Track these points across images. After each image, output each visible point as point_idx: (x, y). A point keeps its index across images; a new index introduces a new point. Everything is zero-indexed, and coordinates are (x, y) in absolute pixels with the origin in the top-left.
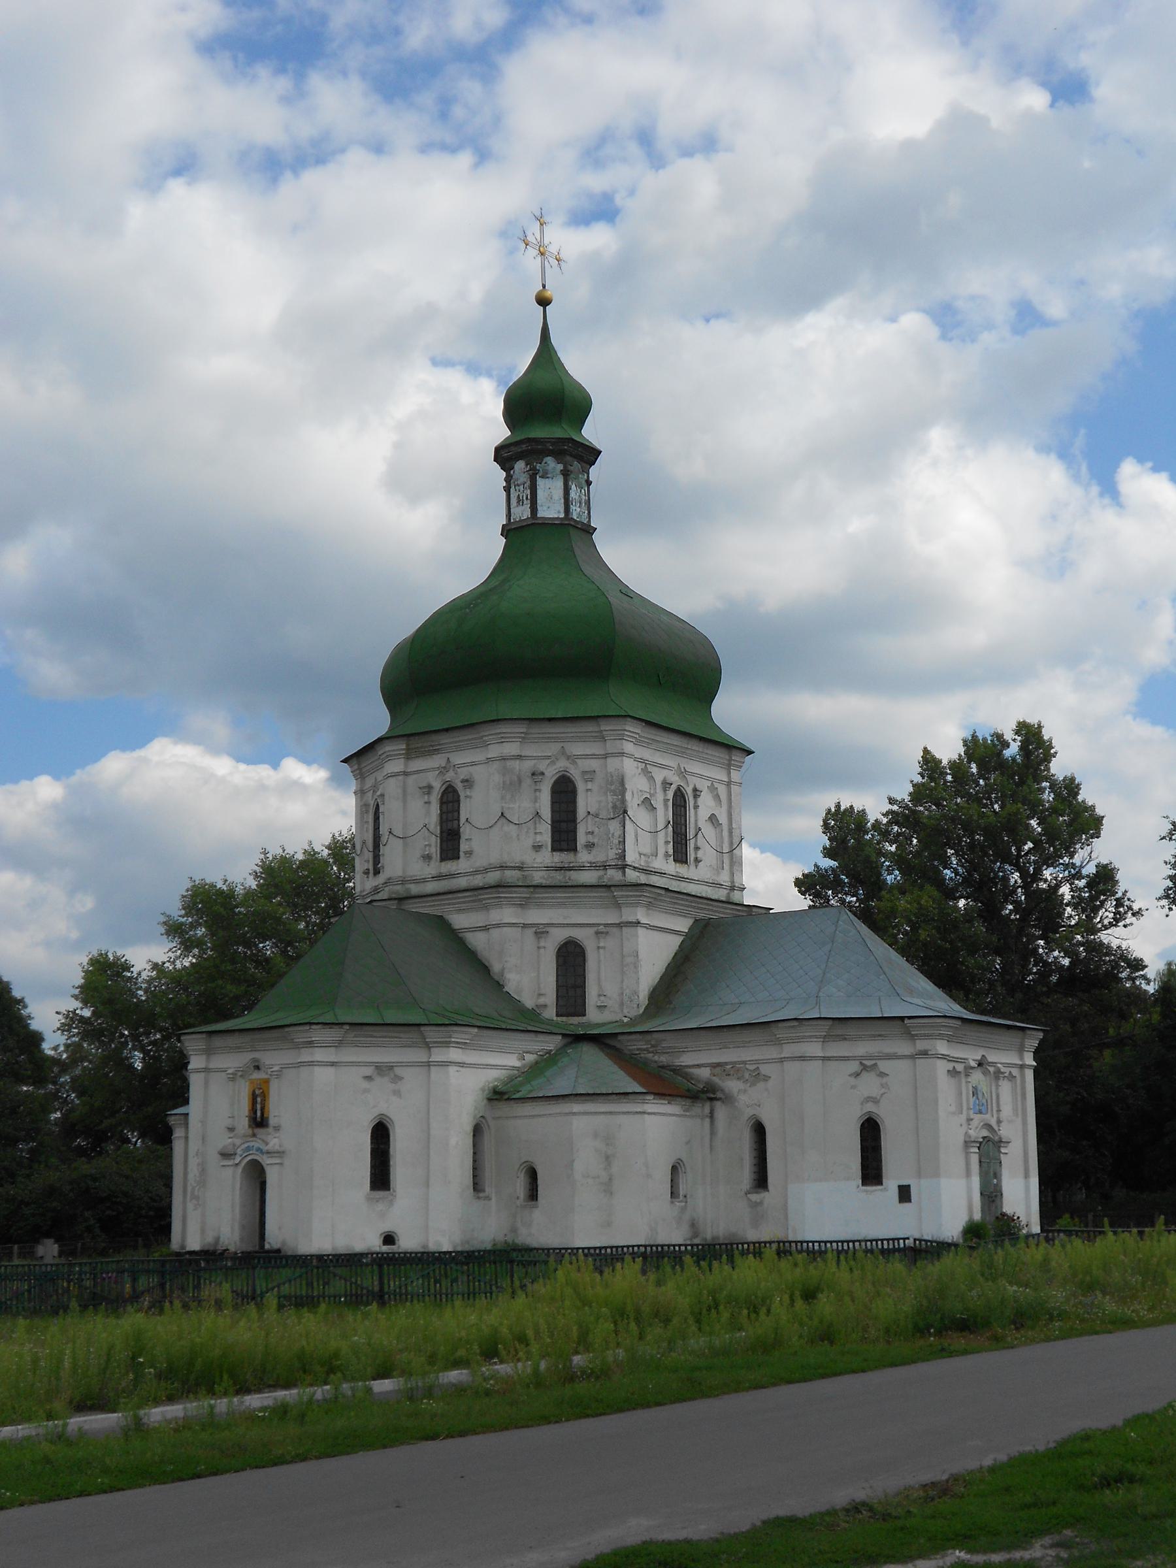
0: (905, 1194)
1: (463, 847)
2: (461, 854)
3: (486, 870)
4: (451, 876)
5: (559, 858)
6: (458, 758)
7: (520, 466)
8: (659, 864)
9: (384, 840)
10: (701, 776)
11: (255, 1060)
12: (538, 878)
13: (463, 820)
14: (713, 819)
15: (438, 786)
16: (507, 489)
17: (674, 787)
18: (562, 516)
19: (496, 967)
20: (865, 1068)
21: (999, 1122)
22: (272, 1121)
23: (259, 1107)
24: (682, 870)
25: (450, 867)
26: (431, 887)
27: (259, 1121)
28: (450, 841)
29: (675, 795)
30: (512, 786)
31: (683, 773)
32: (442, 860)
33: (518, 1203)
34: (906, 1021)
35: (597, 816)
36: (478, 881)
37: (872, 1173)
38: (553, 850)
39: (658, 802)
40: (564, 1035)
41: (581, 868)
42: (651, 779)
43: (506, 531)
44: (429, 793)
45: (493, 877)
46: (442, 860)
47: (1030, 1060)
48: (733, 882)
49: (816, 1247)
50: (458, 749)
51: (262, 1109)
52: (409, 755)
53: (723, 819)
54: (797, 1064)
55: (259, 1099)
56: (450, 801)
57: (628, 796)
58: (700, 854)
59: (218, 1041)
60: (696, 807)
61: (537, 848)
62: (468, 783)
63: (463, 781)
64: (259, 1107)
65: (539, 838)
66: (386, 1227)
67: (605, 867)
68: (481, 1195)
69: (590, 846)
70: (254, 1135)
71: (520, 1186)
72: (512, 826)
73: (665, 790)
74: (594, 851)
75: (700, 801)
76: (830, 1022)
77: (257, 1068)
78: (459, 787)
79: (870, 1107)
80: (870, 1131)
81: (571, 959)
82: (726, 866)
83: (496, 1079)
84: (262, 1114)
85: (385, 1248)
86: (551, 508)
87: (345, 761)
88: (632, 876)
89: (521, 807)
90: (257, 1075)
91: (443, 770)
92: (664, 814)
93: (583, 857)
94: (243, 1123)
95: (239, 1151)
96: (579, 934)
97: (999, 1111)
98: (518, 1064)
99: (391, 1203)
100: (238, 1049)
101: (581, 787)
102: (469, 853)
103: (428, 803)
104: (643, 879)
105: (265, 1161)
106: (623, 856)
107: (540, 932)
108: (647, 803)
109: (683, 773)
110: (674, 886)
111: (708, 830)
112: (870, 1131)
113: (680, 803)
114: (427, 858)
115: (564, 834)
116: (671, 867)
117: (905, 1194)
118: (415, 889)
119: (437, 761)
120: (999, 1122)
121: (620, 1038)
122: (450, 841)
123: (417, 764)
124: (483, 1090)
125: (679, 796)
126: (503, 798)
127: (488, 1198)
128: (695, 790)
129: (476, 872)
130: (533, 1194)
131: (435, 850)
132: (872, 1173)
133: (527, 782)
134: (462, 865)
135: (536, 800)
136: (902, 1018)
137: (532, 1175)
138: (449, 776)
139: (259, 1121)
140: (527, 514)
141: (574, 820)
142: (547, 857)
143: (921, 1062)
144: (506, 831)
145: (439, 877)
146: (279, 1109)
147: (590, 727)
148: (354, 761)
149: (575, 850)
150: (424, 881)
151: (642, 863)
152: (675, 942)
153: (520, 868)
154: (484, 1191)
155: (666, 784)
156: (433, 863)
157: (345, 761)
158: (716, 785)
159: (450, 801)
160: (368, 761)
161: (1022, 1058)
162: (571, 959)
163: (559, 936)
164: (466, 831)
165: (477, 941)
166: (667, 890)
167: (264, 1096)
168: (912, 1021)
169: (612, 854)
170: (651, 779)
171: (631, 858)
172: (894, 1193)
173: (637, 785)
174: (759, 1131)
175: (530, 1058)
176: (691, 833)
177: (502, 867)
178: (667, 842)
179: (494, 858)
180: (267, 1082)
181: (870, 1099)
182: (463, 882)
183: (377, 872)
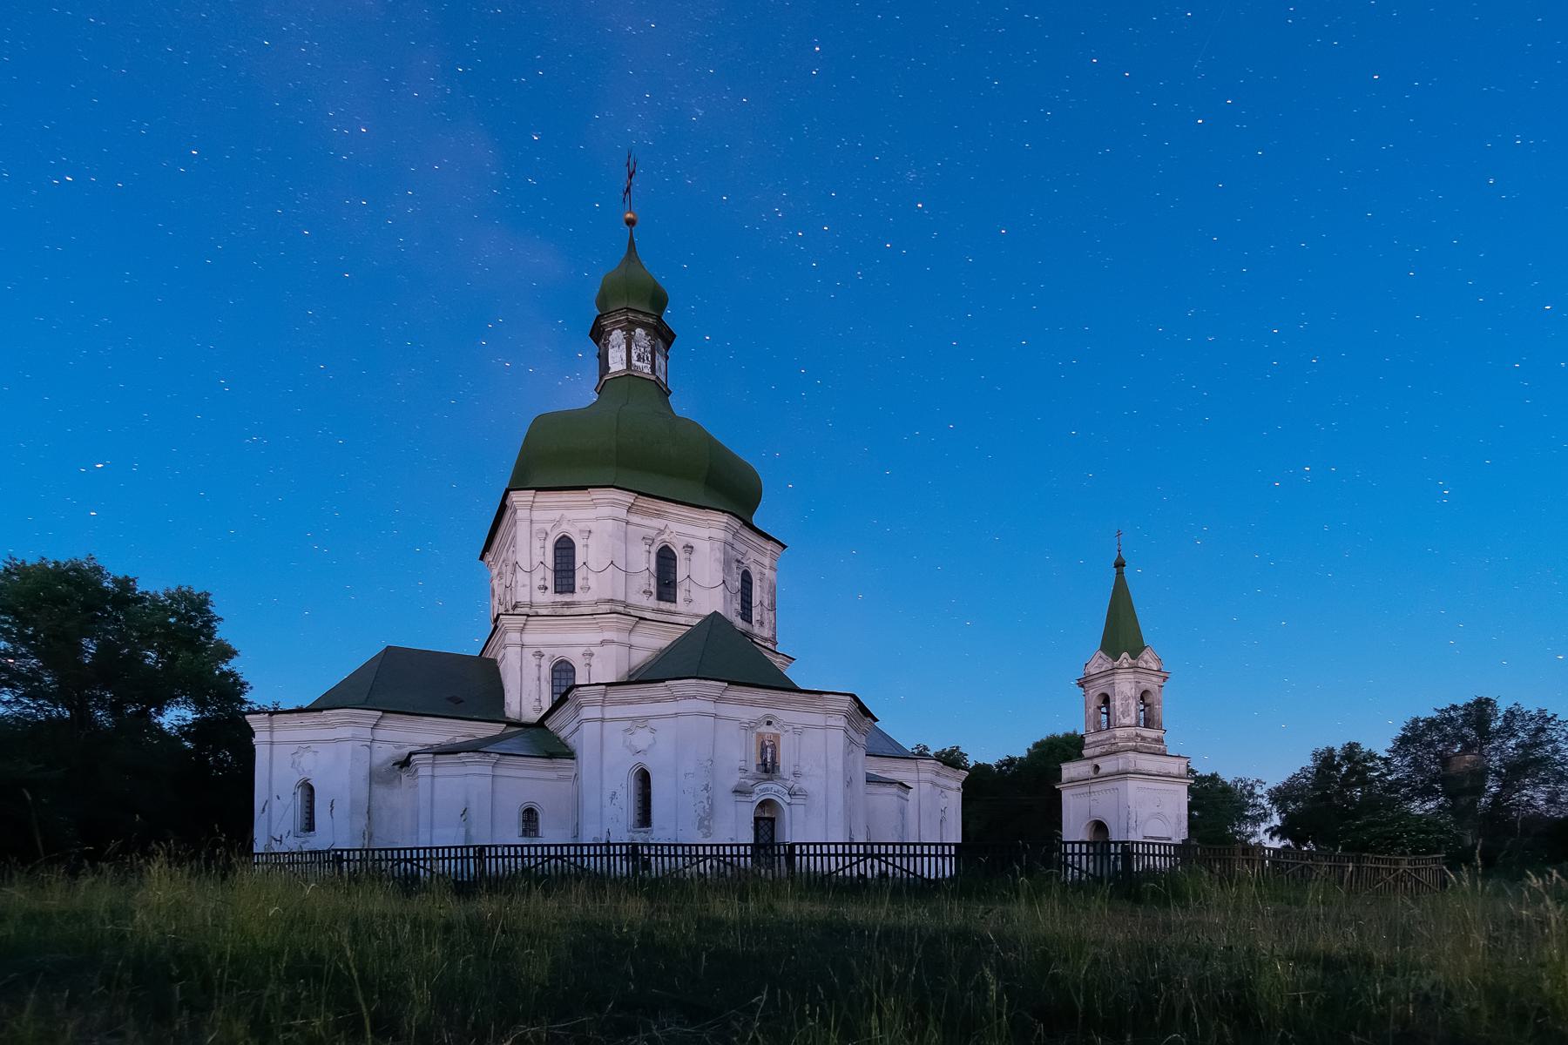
6: (674, 527)
11: (768, 716)
26: (647, 615)
50: (679, 521)
51: (773, 759)
62: (689, 548)
77: (769, 723)
84: (773, 759)
90: (764, 729)
91: (661, 532)
94: (754, 769)
95: (757, 789)
100: (753, 703)
105: (783, 800)
114: (648, 593)
119: (658, 523)
123: (634, 519)
131: (654, 590)
139: (769, 768)
142: (739, 623)
150: (643, 609)
167: (774, 747)
180: (777, 736)
182: (681, 620)
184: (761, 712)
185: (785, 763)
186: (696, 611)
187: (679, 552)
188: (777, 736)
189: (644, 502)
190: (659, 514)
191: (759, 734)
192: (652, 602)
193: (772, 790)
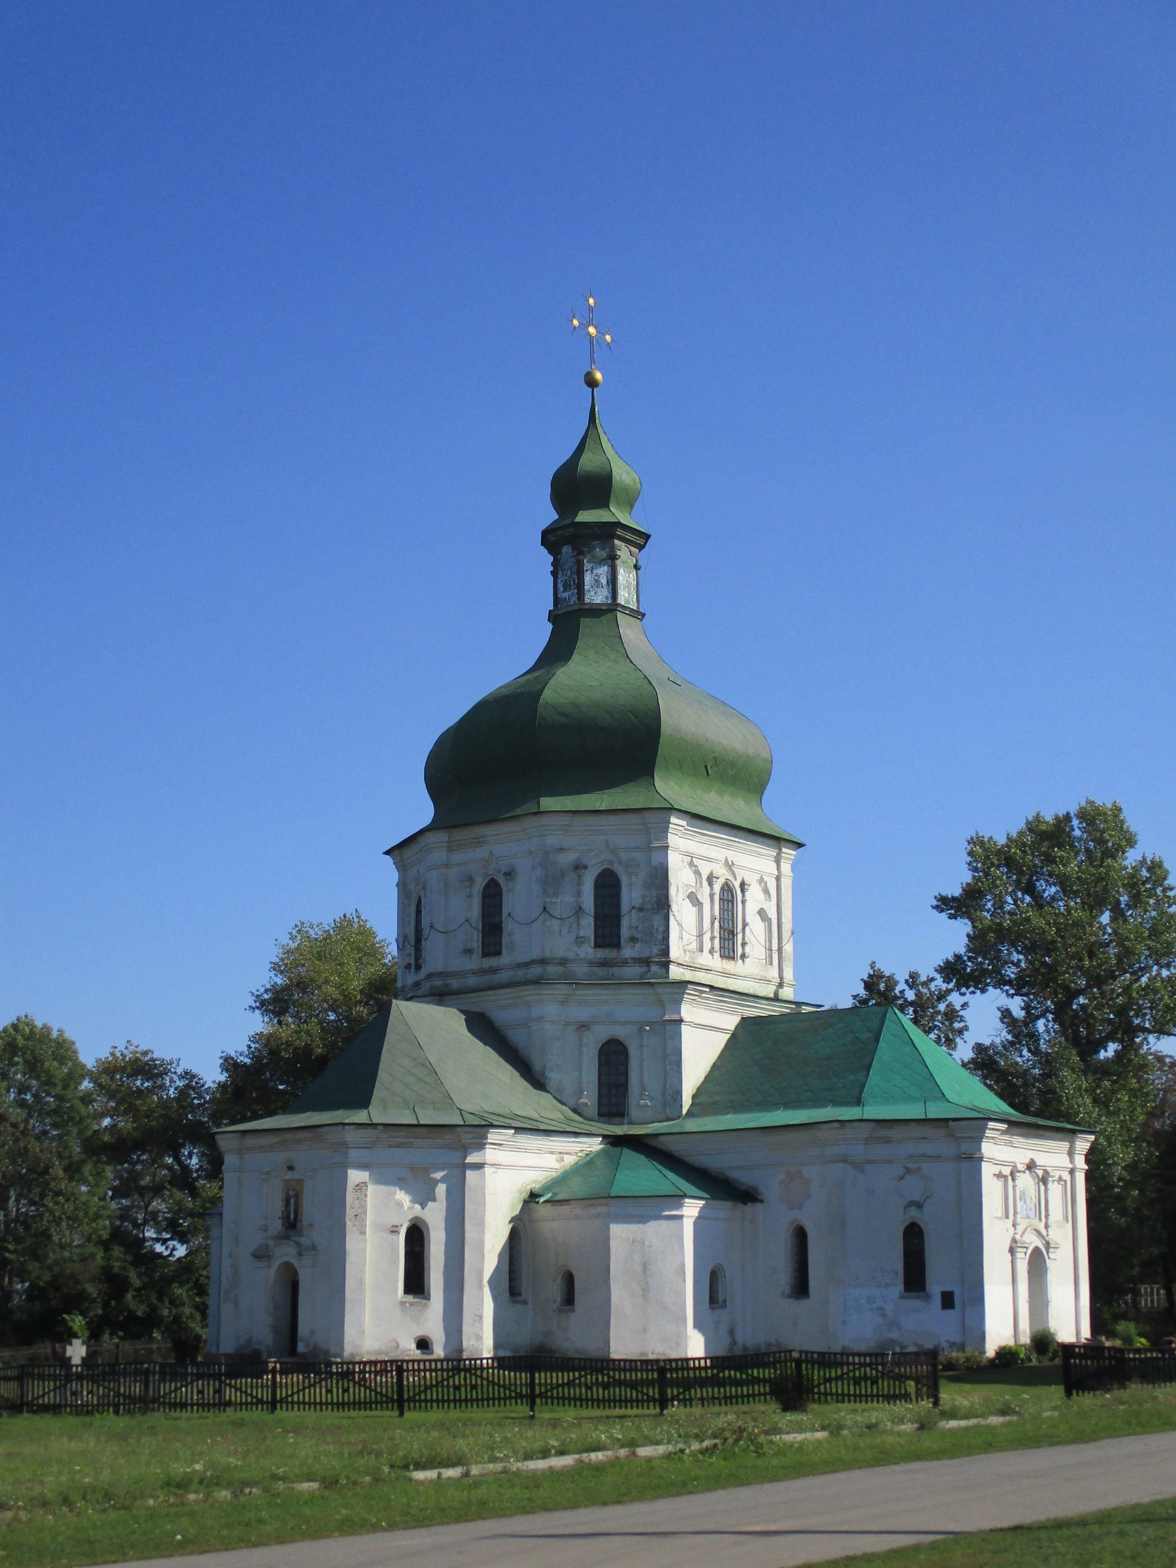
0: (948, 1300)
3: (527, 965)
4: (494, 971)
5: (602, 954)
7: (566, 549)
8: (705, 959)
9: (425, 933)
10: (750, 870)
12: (581, 970)
14: (762, 913)
15: (480, 884)
16: (554, 574)
17: (721, 881)
18: (610, 601)
19: (537, 1065)
20: (908, 1171)
21: (1047, 1226)
22: (305, 1222)
23: (292, 1207)
24: (729, 966)
26: (472, 981)
27: (292, 1224)
29: (722, 889)
30: (552, 881)
31: (729, 866)
32: (485, 954)
33: (555, 1306)
34: (951, 1123)
35: (641, 909)
36: (521, 974)
37: (914, 1279)
38: (597, 945)
39: (704, 895)
40: (604, 1137)
41: (625, 963)
42: (697, 873)
43: (553, 617)
44: (471, 887)
45: (535, 971)
46: (485, 954)
47: (1081, 1163)
48: (781, 978)
49: (674, 1365)
52: (450, 850)
53: (773, 914)
54: (840, 1166)
55: (292, 1201)
56: (492, 895)
57: (672, 891)
58: (747, 949)
59: (250, 1141)
60: (743, 902)
61: (580, 941)
62: (510, 874)
63: (505, 874)
64: (292, 1207)
65: (582, 933)
66: (420, 1332)
67: (646, 962)
68: (518, 1298)
69: (633, 940)
70: (288, 1237)
71: (554, 1291)
72: (556, 922)
73: (711, 884)
74: (638, 946)
75: (747, 894)
76: (874, 1124)
77: (291, 1168)
78: (501, 880)
79: (913, 1213)
80: (913, 1236)
81: (613, 1057)
82: (775, 962)
83: (534, 1182)
85: (417, 1354)
86: (597, 596)
87: (387, 853)
88: (675, 973)
89: (563, 901)
90: (289, 1176)
92: (711, 909)
93: (627, 952)
94: (277, 1226)
96: (620, 1033)
97: (1047, 1216)
98: (556, 1165)
99: (426, 1306)
101: (624, 880)
103: (470, 896)
104: (688, 975)
106: (666, 952)
107: (584, 1026)
108: (693, 898)
109: (729, 866)
110: (720, 982)
111: (756, 928)
112: (913, 1236)
113: (728, 897)
114: (469, 951)
115: (608, 928)
116: (716, 962)
117: (948, 1300)
118: (455, 983)
119: (481, 853)
120: (1047, 1226)
121: (661, 1138)
123: (458, 857)
124: (520, 1192)
125: (727, 888)
126: (545, 892)
127: (525, 1302)
128: (743, 885)
129: (519, 966)
130: (569, 1299)
132: (914, 1279)
133: (572, 876)
134: (505, 959)
135: (579, 894)
136: (947, 1120)
137: (569, 1279)
139: (292, 1224)
140: (574, 599)
141: (618, 917)
142: (588, 951)
143: (964, 1165)
144: (547, 928)
145: (483, 972)
146: (310, 1211)
147: (633, 819)
148: (396, 852)
149: (617, 945)
151: (686, 959)
152: (722, 1040)
153: (563, 962)
154: (520, 1295)
155: (711, 879)
156: (475, 957)
157: (387, 853)
158: (765, 878)
160: (409, 852)
161: (1072, 1161)
162: (613, 1057)
163: (602, 1033)
164: (508, 926)
166: (711, 987)
167: (297, 1196)
168: (955, 1123)
169: (655, 950)
170: (697, 873)
171: (675, 953)
172: (937, 1301)
173: (680, 879)
174: (801, 1236)
175: (570, 1160)
177: (543, 961)
178: (712, 939)
179: (536, 954)
180: (301, 1181)
181: (911, 1204)
182: (504, 976)
183: (418, 967)
184: (280, 1157)
185: (305, 1220)
186: (520, 960)
188: (301, 1181)
189: (461, 835)
190: (479, 842)
191: (285, 1181)
192: (475, 962)
193: (286, 1253)
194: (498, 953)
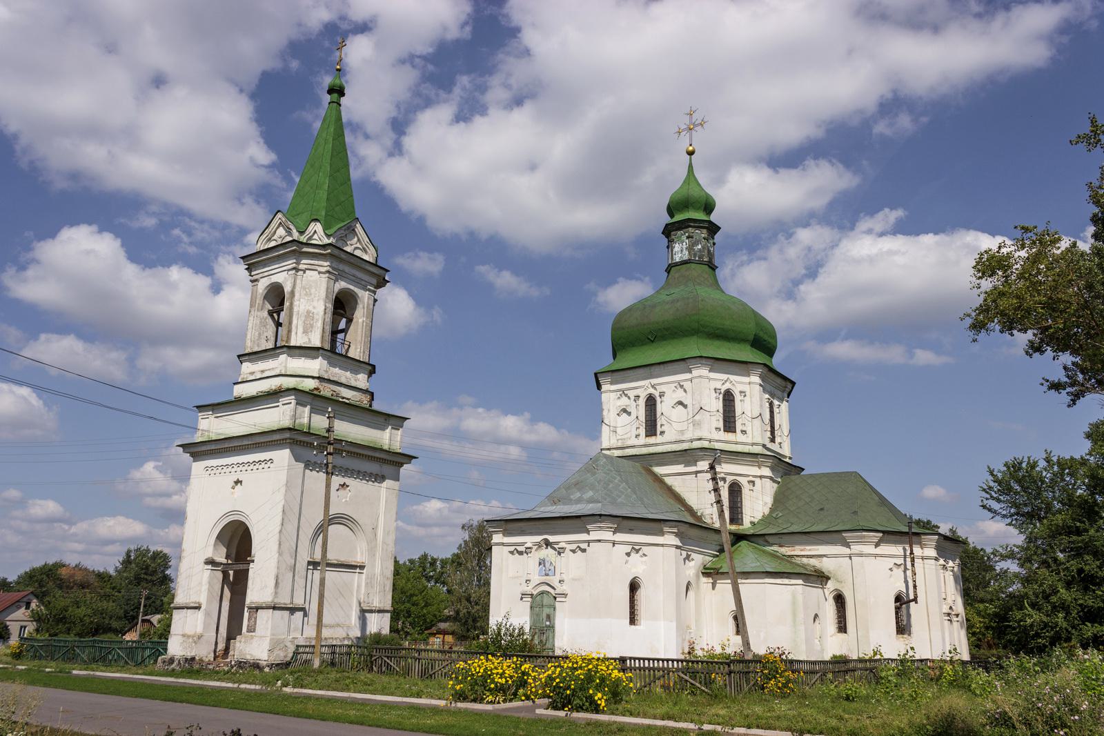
1: (659, 429)
2: (658, 433)
13: (658, 414)
15: (643, 395)
25: (652, 440)
28: (651, 427)
32: (646, 436)
56: (651, 403)
62: (662, 395)
78: (657, 394)
102: (662, 433)
122: (651, 427)
131: (642, 431)
134: (658, 439)
138: (651, 391)
145: (645, 446)
159: (651, 403)
165: (668, 481)
176: (777, 427)
187: (658, 400)
192: (643, 440)
194: (655, 435)
